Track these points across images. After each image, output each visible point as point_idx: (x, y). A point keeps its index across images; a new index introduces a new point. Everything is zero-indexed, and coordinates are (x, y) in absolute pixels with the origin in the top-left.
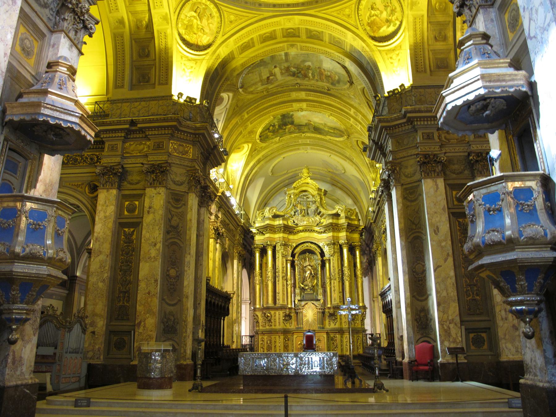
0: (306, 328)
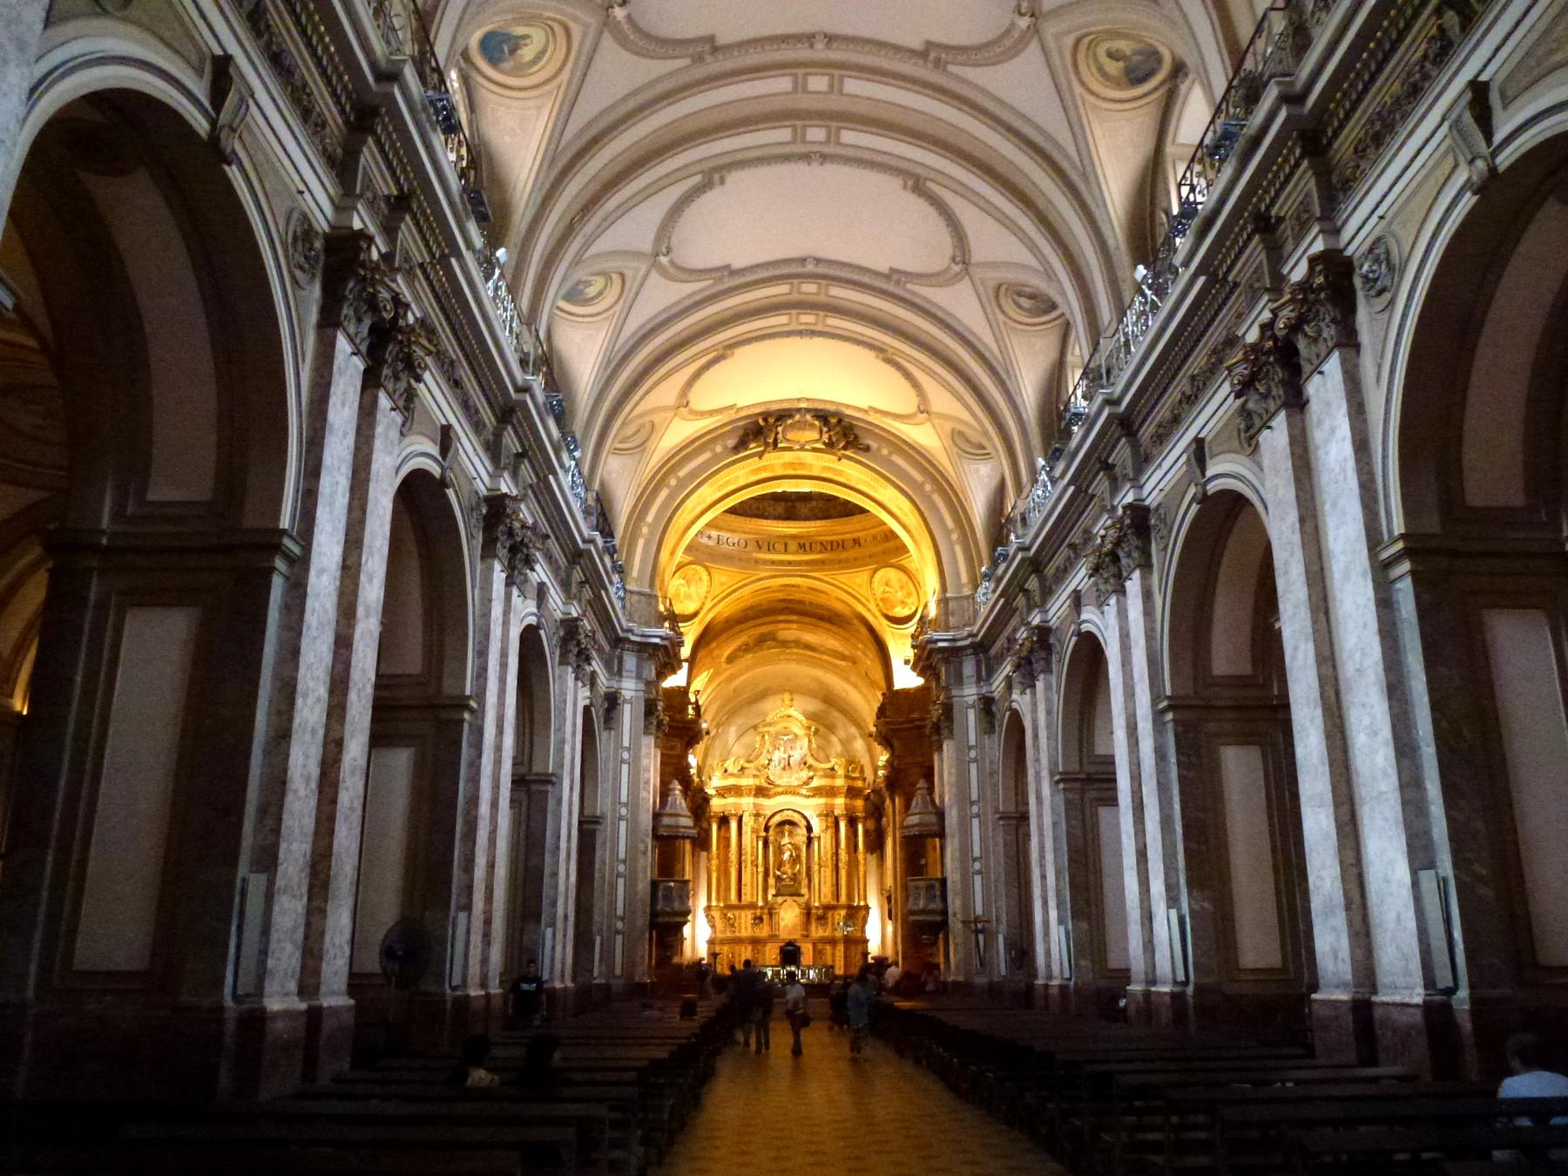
0: (785, 935)
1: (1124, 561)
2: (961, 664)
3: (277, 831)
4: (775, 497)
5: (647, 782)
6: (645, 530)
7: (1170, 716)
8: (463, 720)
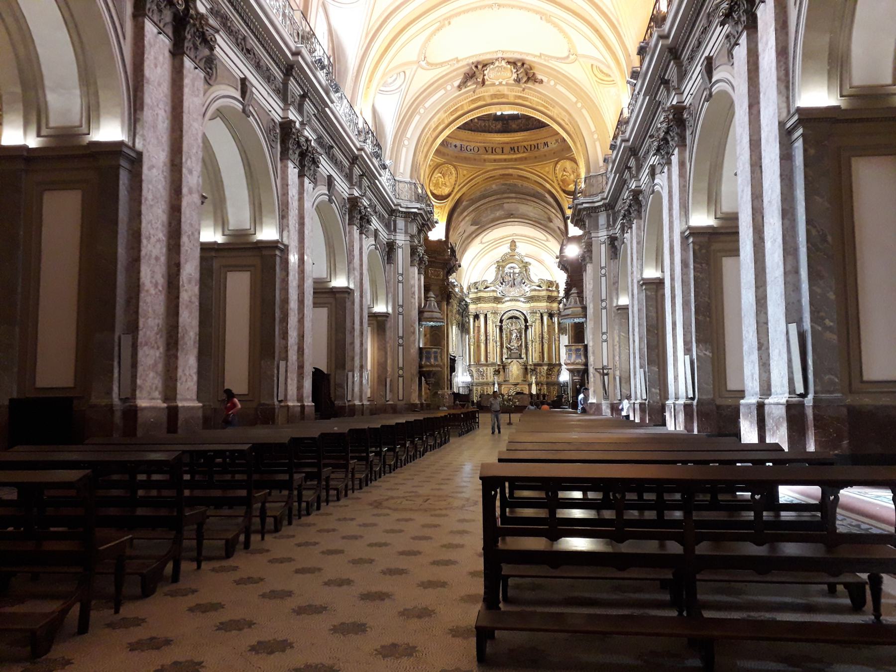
1: (671, 143)
2: (598, 216)
3: (137, 312)
4: (496, 118)
5: (414, 293)
6: (406, 142)
7: (691, 240)
8: (275, 255)
